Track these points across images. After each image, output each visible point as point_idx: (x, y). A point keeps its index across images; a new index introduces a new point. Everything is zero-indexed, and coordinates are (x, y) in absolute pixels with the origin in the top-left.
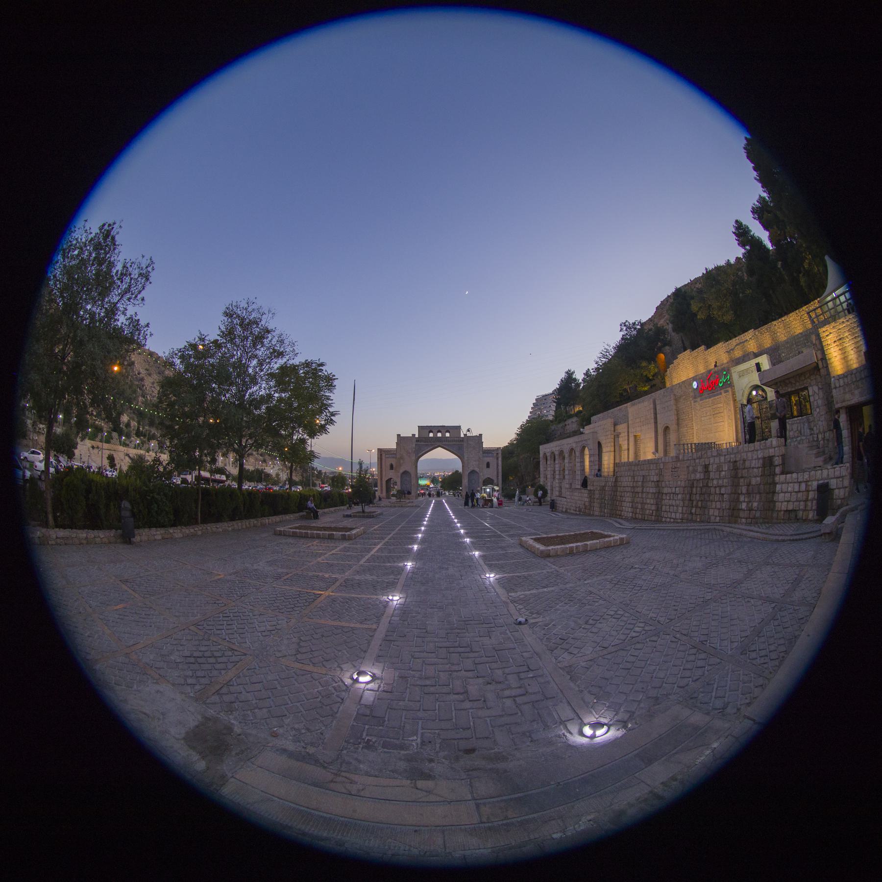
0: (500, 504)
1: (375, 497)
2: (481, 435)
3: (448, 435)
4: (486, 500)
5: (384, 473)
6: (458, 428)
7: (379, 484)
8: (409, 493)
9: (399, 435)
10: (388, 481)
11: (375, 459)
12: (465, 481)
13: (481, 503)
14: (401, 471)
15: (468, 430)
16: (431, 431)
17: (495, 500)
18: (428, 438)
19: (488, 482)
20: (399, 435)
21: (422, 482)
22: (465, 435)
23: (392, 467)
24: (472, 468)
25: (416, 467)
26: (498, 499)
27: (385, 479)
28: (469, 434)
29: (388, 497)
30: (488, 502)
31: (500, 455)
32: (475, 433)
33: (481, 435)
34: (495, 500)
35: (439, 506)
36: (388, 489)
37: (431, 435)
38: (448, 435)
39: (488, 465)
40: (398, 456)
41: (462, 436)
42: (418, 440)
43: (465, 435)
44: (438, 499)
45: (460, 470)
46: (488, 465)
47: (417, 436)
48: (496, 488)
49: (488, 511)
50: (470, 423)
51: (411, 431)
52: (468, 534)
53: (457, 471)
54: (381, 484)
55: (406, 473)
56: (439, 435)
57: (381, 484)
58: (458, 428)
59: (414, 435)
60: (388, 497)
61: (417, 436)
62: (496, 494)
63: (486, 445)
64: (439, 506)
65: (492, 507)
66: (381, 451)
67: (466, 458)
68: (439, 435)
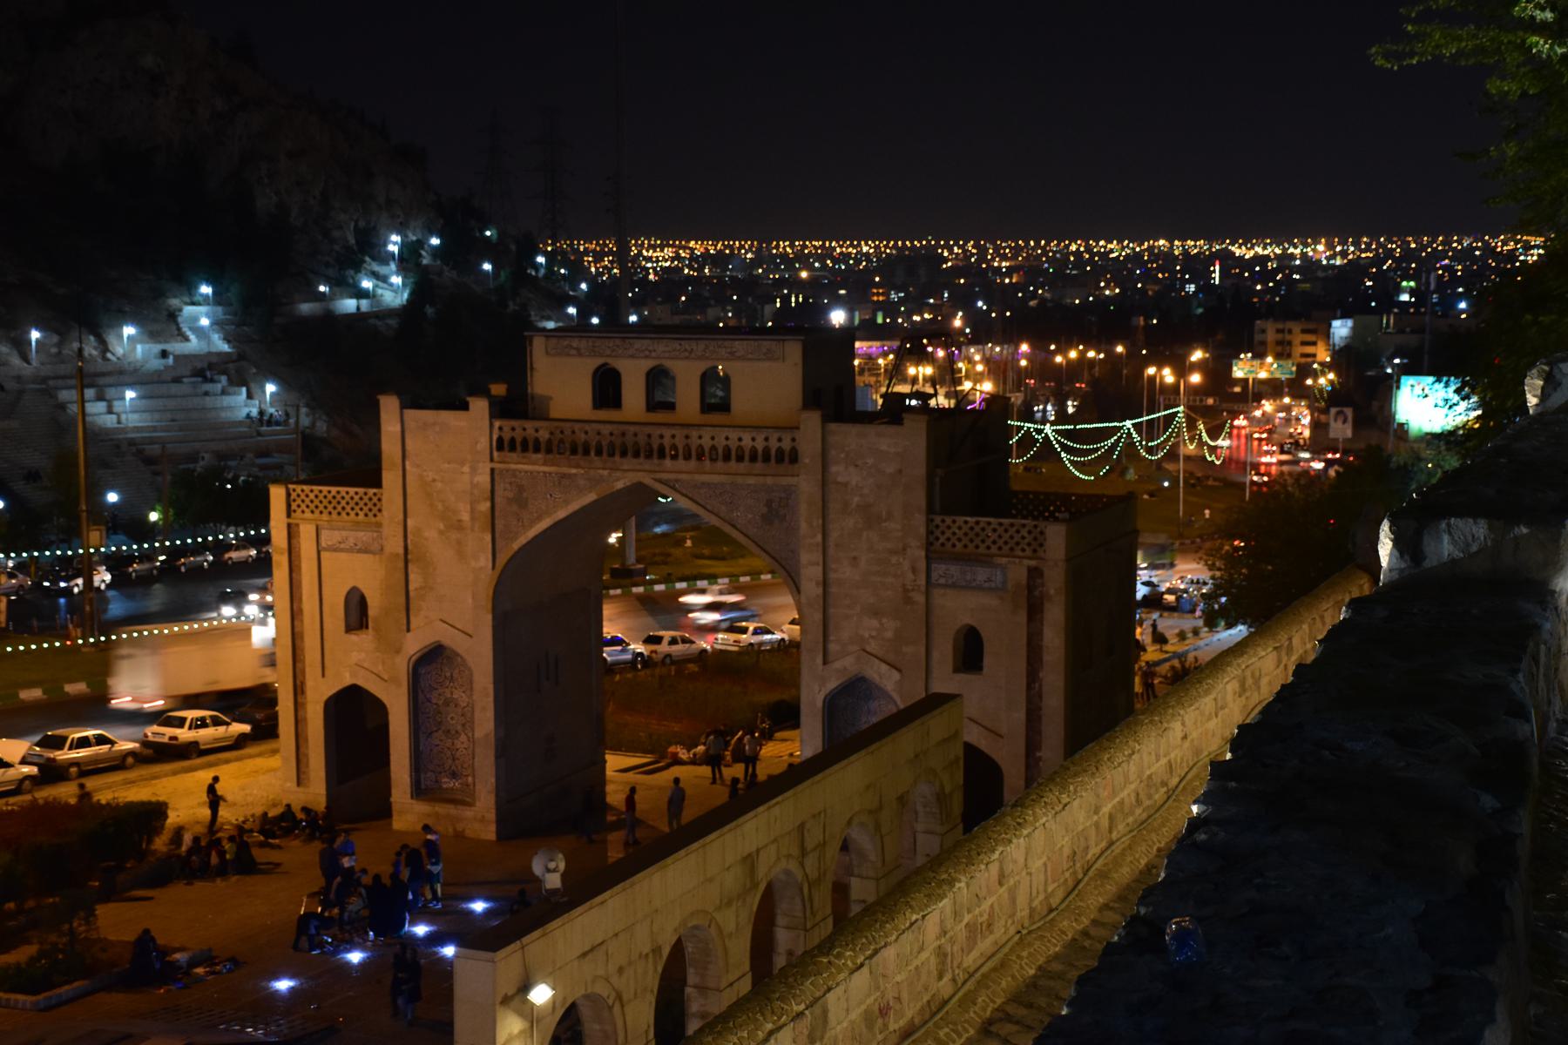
14: (414, 644)
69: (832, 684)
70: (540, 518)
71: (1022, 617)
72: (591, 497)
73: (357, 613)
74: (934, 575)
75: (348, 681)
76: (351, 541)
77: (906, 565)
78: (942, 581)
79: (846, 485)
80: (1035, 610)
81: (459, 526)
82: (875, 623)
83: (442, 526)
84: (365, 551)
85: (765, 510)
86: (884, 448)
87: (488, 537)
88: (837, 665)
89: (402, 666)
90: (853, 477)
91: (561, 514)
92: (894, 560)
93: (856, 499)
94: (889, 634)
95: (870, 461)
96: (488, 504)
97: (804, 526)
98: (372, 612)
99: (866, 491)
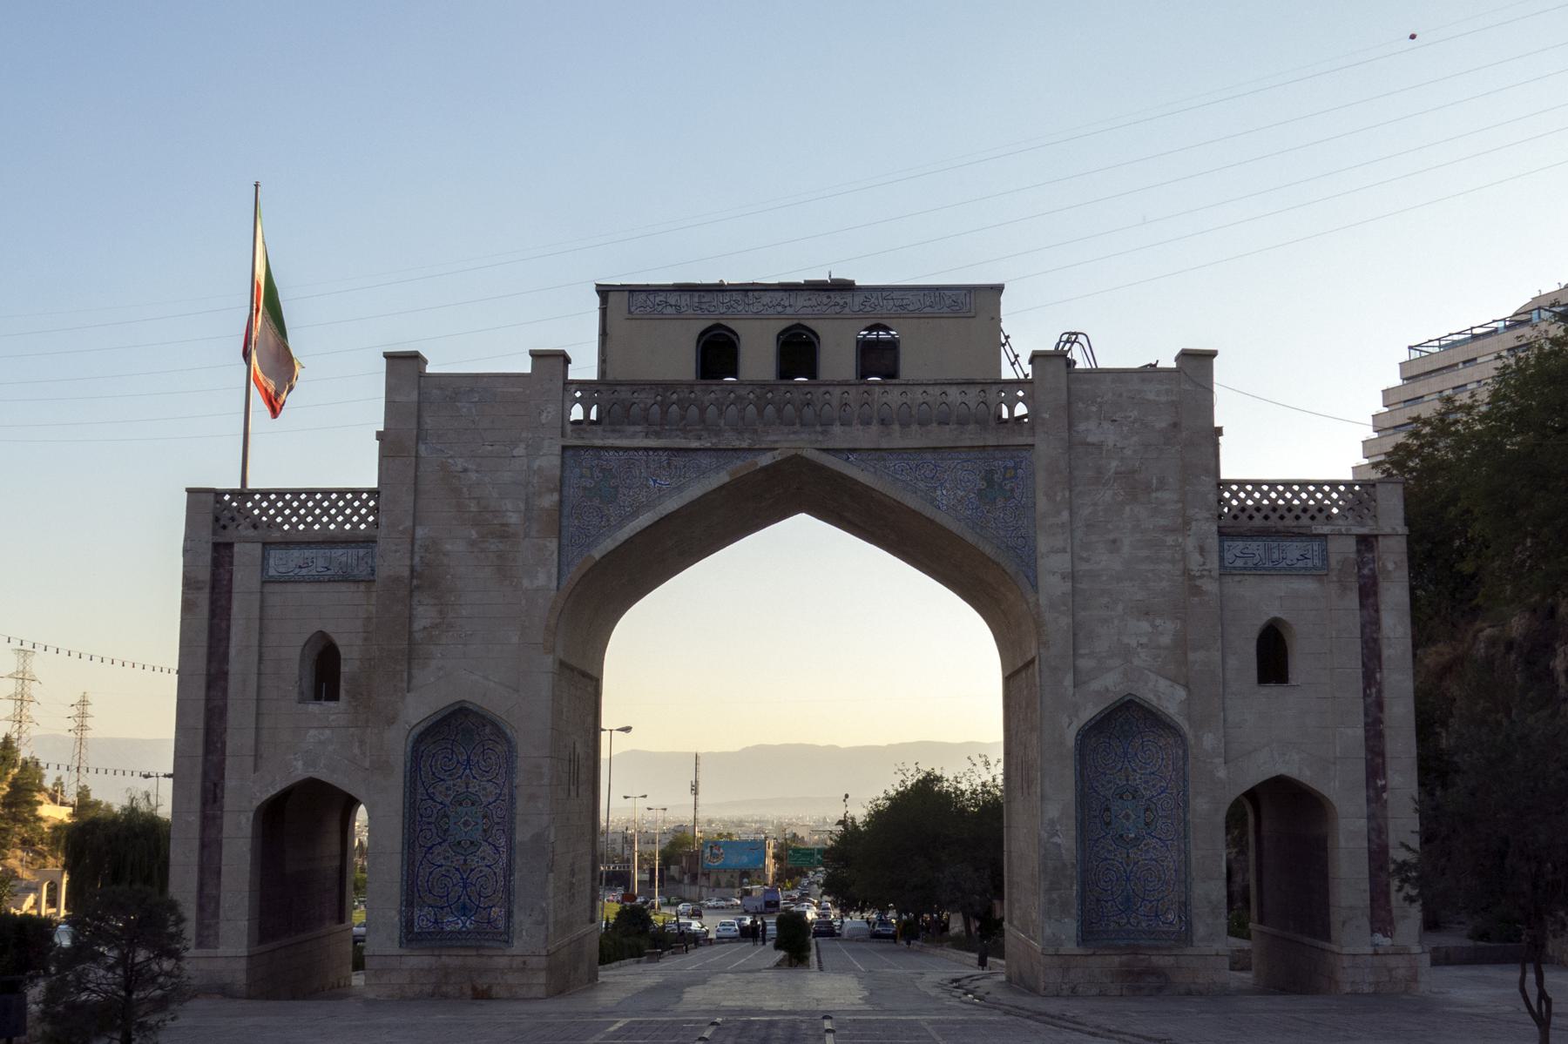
2: (1197, 363)
5: (238, 738)
14: (418, 708)
24: (1110, 684)
31: (1393, 558)
33: (1197, 363)
39: (1272, 656)
40: (392, 562)
46: (1272, 656)
47: (584, 367)
51: (523, 314)
55: (459, 732)
59: (552, 361)
61: (584, 367)
67: (1052, 585)
69: (1089, 712)
70: (635, 514)
71: (1353, 600)
72: (723, 478)
73: (325, 671)
74: (1228, 556)
75: (299, 771)
76: (321, 562)
77: (1190, 544)
78: (1239, 563)
79: (1099, 446)
80: (1368, 592)
81: (504, 534)
82: (1145, 626)
83: (474, 534)
84: (346, 578)
85: (983, 485)
86: (1151, 397)
87: (553, 545)
88: (1095, 685)
89: (397, 743)
90: (1107, 435)
91: (671, 505)
92: (1170, 540)
93: (1114, 464)
94: (1166, 640)
95: (1134, 414)
96: (556, 497)
97: (1042, 503)
98: (348, 668)
99: (1128, 452)
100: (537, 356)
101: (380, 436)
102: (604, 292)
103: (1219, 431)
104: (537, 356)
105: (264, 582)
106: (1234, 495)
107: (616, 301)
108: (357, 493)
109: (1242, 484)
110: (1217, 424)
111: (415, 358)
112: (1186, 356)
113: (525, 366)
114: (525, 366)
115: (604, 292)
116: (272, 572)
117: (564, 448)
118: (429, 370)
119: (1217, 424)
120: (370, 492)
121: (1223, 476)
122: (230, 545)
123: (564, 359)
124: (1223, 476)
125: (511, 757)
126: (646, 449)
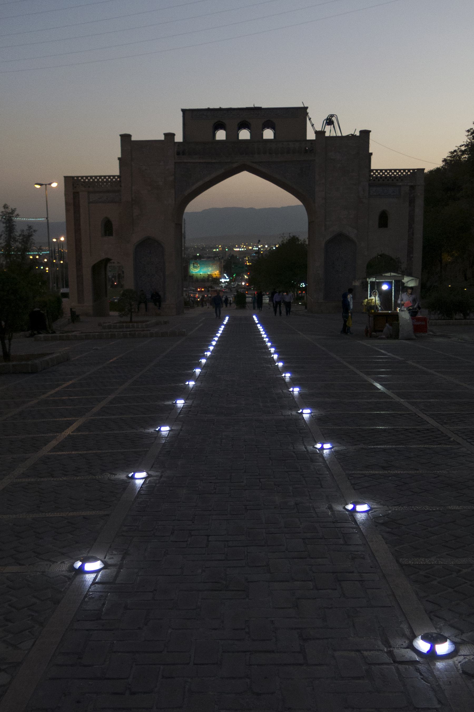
0: (420, 328)
1: (57, 312)
3: (268, 134)
4: (377, 316)
6: (300, 114)
7: (72, 279)
8: (157, 299)
9: (125, 138)
10: (100, 268)
11: (59, 213)
12: (316, 264)
13: (358, 324)
15: (329, 121)
16: (219, 126)
17: (405, 315)
18: (215, 141)
19: (381, 265)
20: (125, 138)
21: (199, 271)
22: (320, 134)
23: (108, 228)
25: (179, 225)
26: (413, 313)
27: (89, 262)
28: (329, 132)
29: (99, 312)
30: (382, 322)
32: (348, 127)
34: (405, 315)
35: (241, 333)
36: (99, 291)
37: (221, 135)
38: (268, 134)
41: (311, 136)
42: (183, 149)
43: (320, 134)
44: (240, 313)
45: (303, 236)
46: (383, 221)
48: (409, 282)
49: (381, 348)
50: (334, 102)
51: (161, 122)
52: (326, 426)
53: (294, 240)
54: (80, 277)
55: (148, 245)
56: (244, 135)
57: (80, 277)
58: (300, 114)
59: (170, 136)
60: (99, 312)
62: (405, 298)
63: (376, 164)
64: (241, 333)
65: (395, 335)
66: (74, 185)
68: (244, 135)
80: (412, 201)
100: (166, 135)
101: (119, 159)
102: (184, 111)
103: (371, 154)
104: (166, 135)
105: (89, 203)
106: (374, 173)
107: (189, 115)
108: (114, 176)
109: (377, 170)
110: (370, 152)
111: (129, 136)
112: (361, 132)
113: (162, 138)
114: (162, 138)
115: (184, 111)
116: (91, 200)
117: (175, 163)
118: (133, 139)
119: (370, 152)
120: (117, 176)
121: (372, 167)
122: (78, 193)
123: (173, 135)
124: (372, 167)
125: (163, 254)
126: (200, 163)
